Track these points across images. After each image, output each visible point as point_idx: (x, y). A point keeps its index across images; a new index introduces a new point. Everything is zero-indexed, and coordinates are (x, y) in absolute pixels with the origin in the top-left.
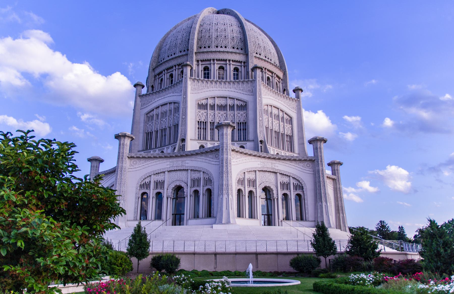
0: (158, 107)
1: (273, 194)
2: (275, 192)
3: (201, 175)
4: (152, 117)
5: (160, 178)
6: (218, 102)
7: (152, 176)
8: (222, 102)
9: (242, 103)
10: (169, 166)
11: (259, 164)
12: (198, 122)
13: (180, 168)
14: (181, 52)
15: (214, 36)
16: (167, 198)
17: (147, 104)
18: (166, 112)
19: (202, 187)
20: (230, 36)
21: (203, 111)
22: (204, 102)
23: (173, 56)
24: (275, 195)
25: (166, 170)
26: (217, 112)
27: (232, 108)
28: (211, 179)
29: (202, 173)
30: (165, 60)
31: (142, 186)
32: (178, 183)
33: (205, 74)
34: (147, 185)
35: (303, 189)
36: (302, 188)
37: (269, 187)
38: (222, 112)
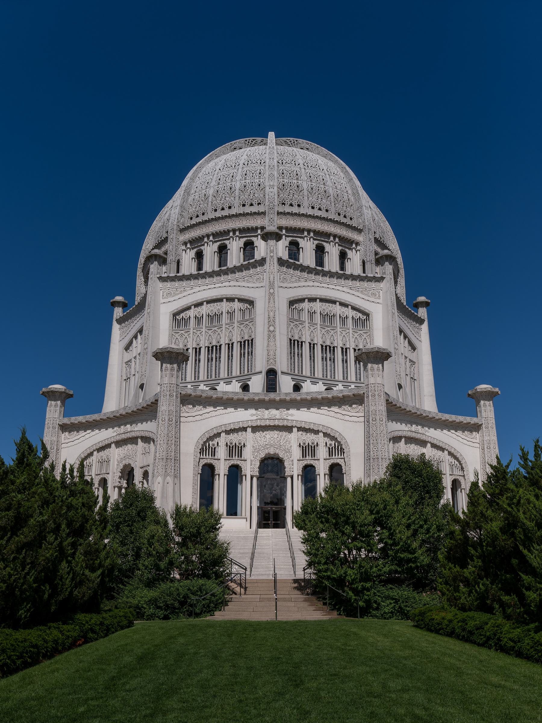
0: (198, 305)
3: (321, 439)
4: (186, 321)
7: (223, 435)
9: (359, 315)
10: (255, 418)
12: (291, 340)
13: (277, 423)
14: (244, 205)
15: (305, 186)
16: (252, 478)
17: (175, 294)
18: (218, 316)
19: (322, 460)
20: (331, 191)
23: (226, 213)
25: (250, 424)
27: (344, 320)
28: (343, 447)
29: (321, 434)
30: (205, 218)
32: (272, 451)
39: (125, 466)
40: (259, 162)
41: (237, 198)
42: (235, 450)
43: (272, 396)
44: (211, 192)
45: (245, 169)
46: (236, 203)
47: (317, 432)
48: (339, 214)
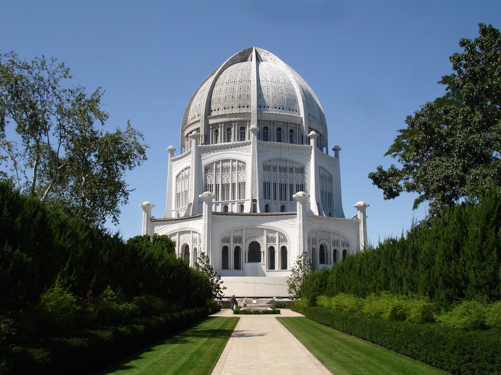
1: (327, 250)
2: (329, 248)
5: (237, 234)
6: (278, 164)
8: (283, 164)
10: (246, 224)
11: (319, 225)
14: (240, 107)
16: (245, 252)
18: (228, 169)
21: (267, 172)
22: (269, 164)
24: (329, 251)
26: (278, 173)
27: (291, 170)
29: (277, 233)
31: (223, 241)
33: (264, 132)
34: (228, 241)
35: (349, 246)
36: (348, 245)
37: (324, 244)
38: (283, 174)
39: (184, 244)
40: (247, 80)
41: (236, 102)
42: (238, 239)
43: (255, 214)
44: (222, 96)
45: (240, 85)
46: (236, 105)
47: (275, 232)
48: (290, 110)
